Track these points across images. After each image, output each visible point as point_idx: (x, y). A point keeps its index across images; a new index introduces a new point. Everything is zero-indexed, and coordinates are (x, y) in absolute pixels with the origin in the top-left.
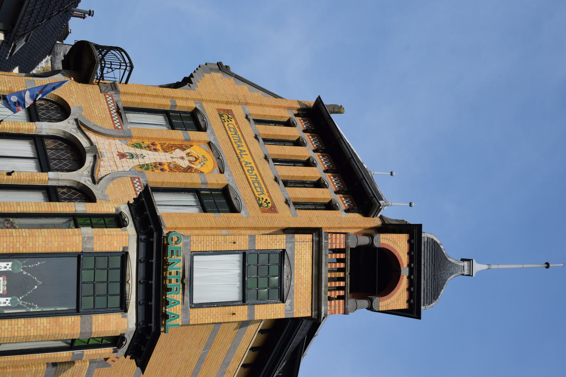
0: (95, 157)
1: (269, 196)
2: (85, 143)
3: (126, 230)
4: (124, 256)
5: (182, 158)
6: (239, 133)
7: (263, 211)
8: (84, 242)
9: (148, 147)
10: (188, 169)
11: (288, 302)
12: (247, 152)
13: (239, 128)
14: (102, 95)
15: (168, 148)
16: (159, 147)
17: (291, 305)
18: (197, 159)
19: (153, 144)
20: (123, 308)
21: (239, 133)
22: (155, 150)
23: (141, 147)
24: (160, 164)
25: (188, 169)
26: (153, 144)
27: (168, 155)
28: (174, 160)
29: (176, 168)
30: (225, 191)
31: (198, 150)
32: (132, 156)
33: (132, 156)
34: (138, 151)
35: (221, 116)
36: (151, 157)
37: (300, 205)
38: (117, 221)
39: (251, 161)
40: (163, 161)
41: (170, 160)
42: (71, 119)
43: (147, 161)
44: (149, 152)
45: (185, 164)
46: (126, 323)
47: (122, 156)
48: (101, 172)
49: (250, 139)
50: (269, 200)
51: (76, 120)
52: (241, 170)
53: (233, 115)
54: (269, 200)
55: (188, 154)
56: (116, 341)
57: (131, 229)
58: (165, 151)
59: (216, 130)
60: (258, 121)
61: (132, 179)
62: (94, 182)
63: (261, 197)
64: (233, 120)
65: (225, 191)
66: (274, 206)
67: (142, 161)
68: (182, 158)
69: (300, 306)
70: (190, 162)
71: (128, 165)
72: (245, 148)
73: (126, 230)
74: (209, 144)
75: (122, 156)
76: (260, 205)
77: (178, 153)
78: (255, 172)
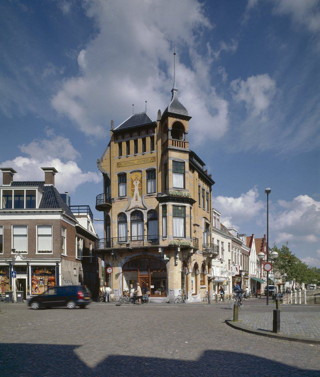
0: (138, 208)
1: (150, 158)
2: (134, 210)
3: (167, 205)
4: (173, 205)
5: (136, 182)
6: (126, 162)
7: (155, 161)
8: (170, 216)
9: (133, 192)
10: (141, 182)
11: (185, 161)
12: (133, 161)
13: (124, 162)
14: (116, 203)
15: (133, 186)
16: (133, 189)
17: (186, 160)
18: (136, 178)
19: (132, 190)
20: (185, 207)
21: (126, 162)
22: (134, 190)
23: (133, 194)
24: (139, 189)
25: (141, 182)
26: (132, 190)
27: (135, 186)
28: (137, 185)
29: (141, 184)
30: (148, 171)
31: (134, 176)
32: (137, 197)
33: (137, 197)
34: (135, 195)
35: (119, 167)
36: (137, 192)
37: (153, 148)
38: (165, 207)
39: (137, 161)
40: (138, 188)
41: (137, 186)
42: (125, 213)
43: (138, 193)
44: (135, 192)
45: (138, 182)
46: (188, 205)
47: (137, 200)
48: (142, 206)
49: (128, 159)
50: (151, 158)
51: (126, 211)
52: (140, 165)
53: (119, 163)
54: (151, 158)
55: (135, 180)
56: (191, 208)
57: (167, 203)
58: (134, 187)
59: (127, 170)
60: (121, 154)
61: (145, 198)
62: (146, 209)
63: (150, 161)
64: (121, 163)
65: (148, 171)
66: (153, 157)
67: (138, 194)
68: (136, 182)
69: (185, 158)
70: (138, 180)
71: (139, 198)
72: (132, 162)
73: (167, 205)
74: (131, 173)
75: (137, 200)
76: (153, 162)
77: (134, 183)
78: (141, 160)
